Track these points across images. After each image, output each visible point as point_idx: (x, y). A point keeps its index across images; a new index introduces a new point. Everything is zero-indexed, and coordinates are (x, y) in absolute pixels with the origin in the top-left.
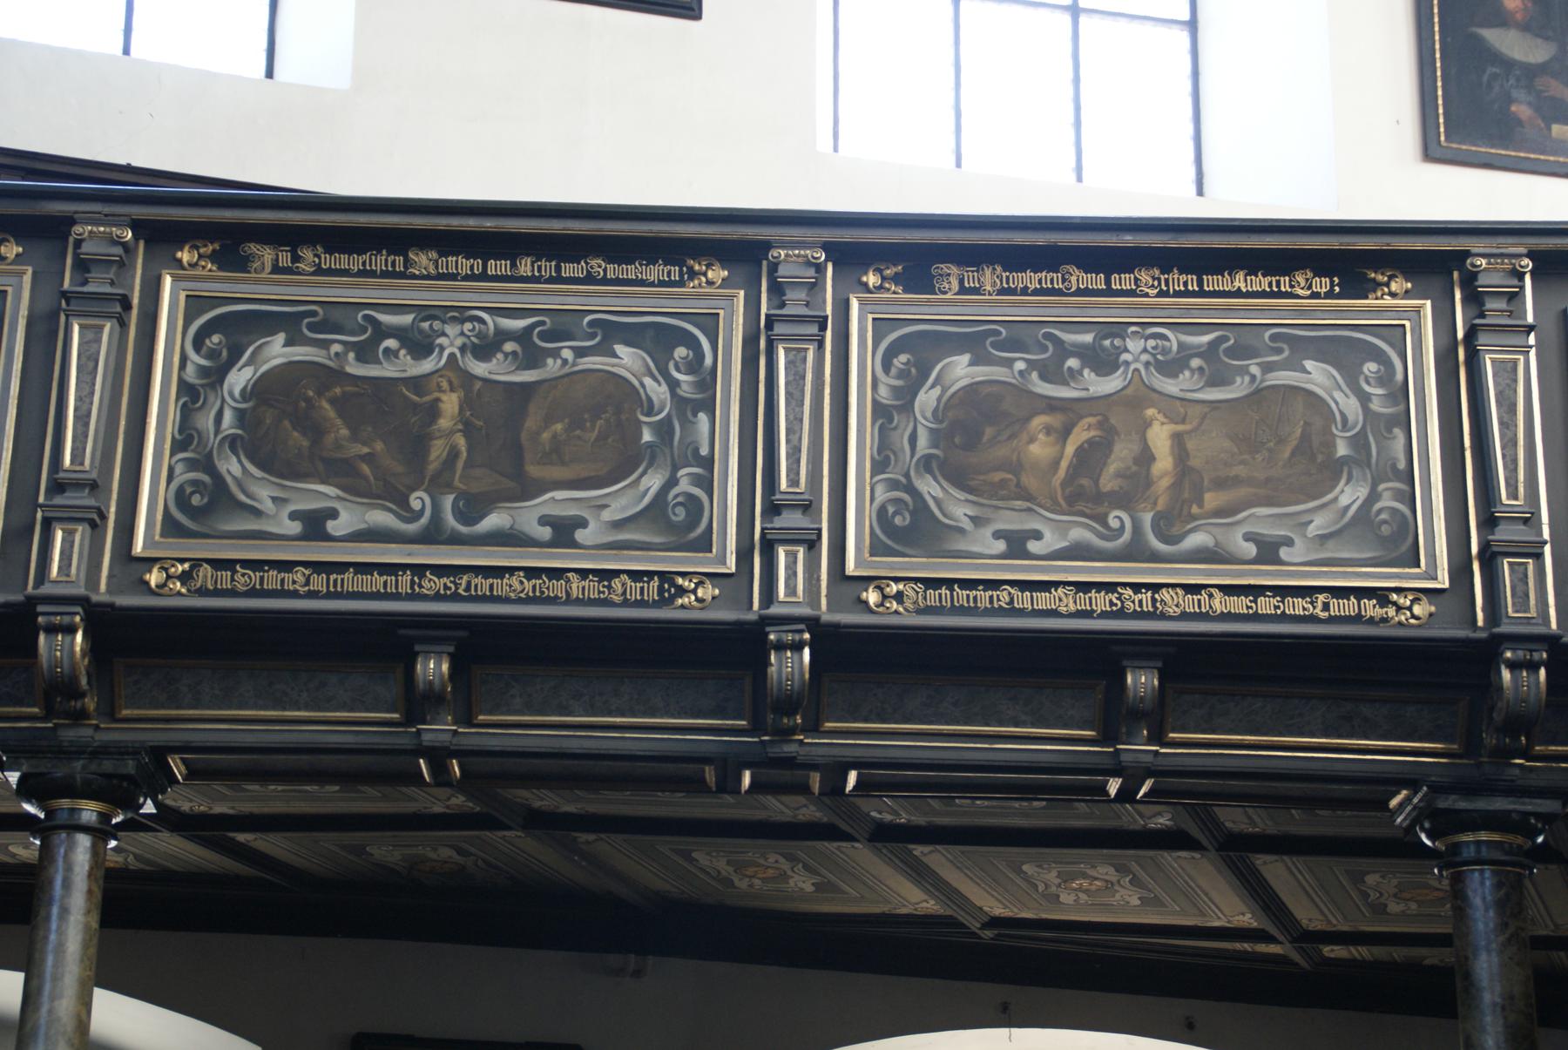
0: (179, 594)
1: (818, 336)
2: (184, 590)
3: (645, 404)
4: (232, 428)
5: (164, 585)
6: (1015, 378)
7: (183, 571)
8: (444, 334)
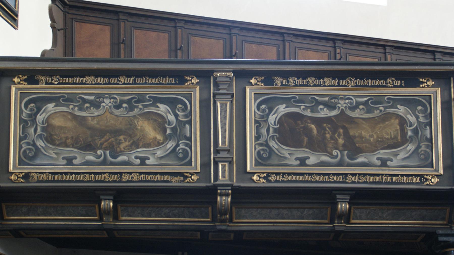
1: (231, 99)
4: (39, 132)
6: (71, 111)
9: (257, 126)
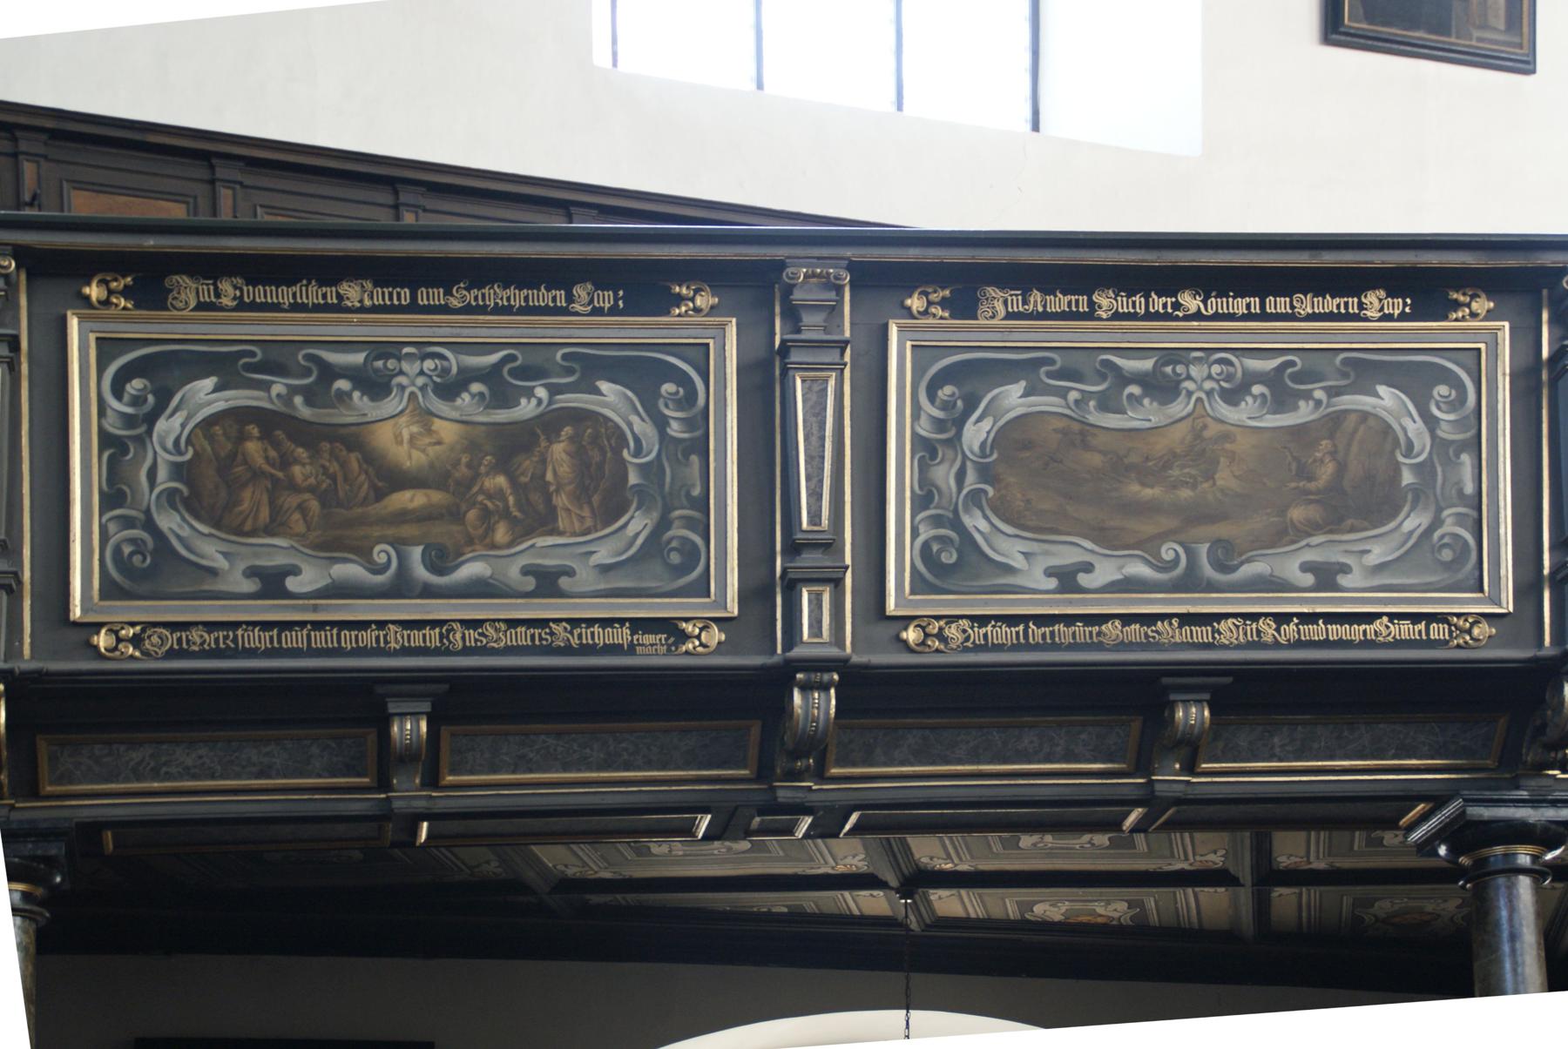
0: (132, 657)
2: (137, 654)
3: (632, 444)
5: (116, 649)
7: (134, 634)
8: (401, 373)
9: (921, 459)
